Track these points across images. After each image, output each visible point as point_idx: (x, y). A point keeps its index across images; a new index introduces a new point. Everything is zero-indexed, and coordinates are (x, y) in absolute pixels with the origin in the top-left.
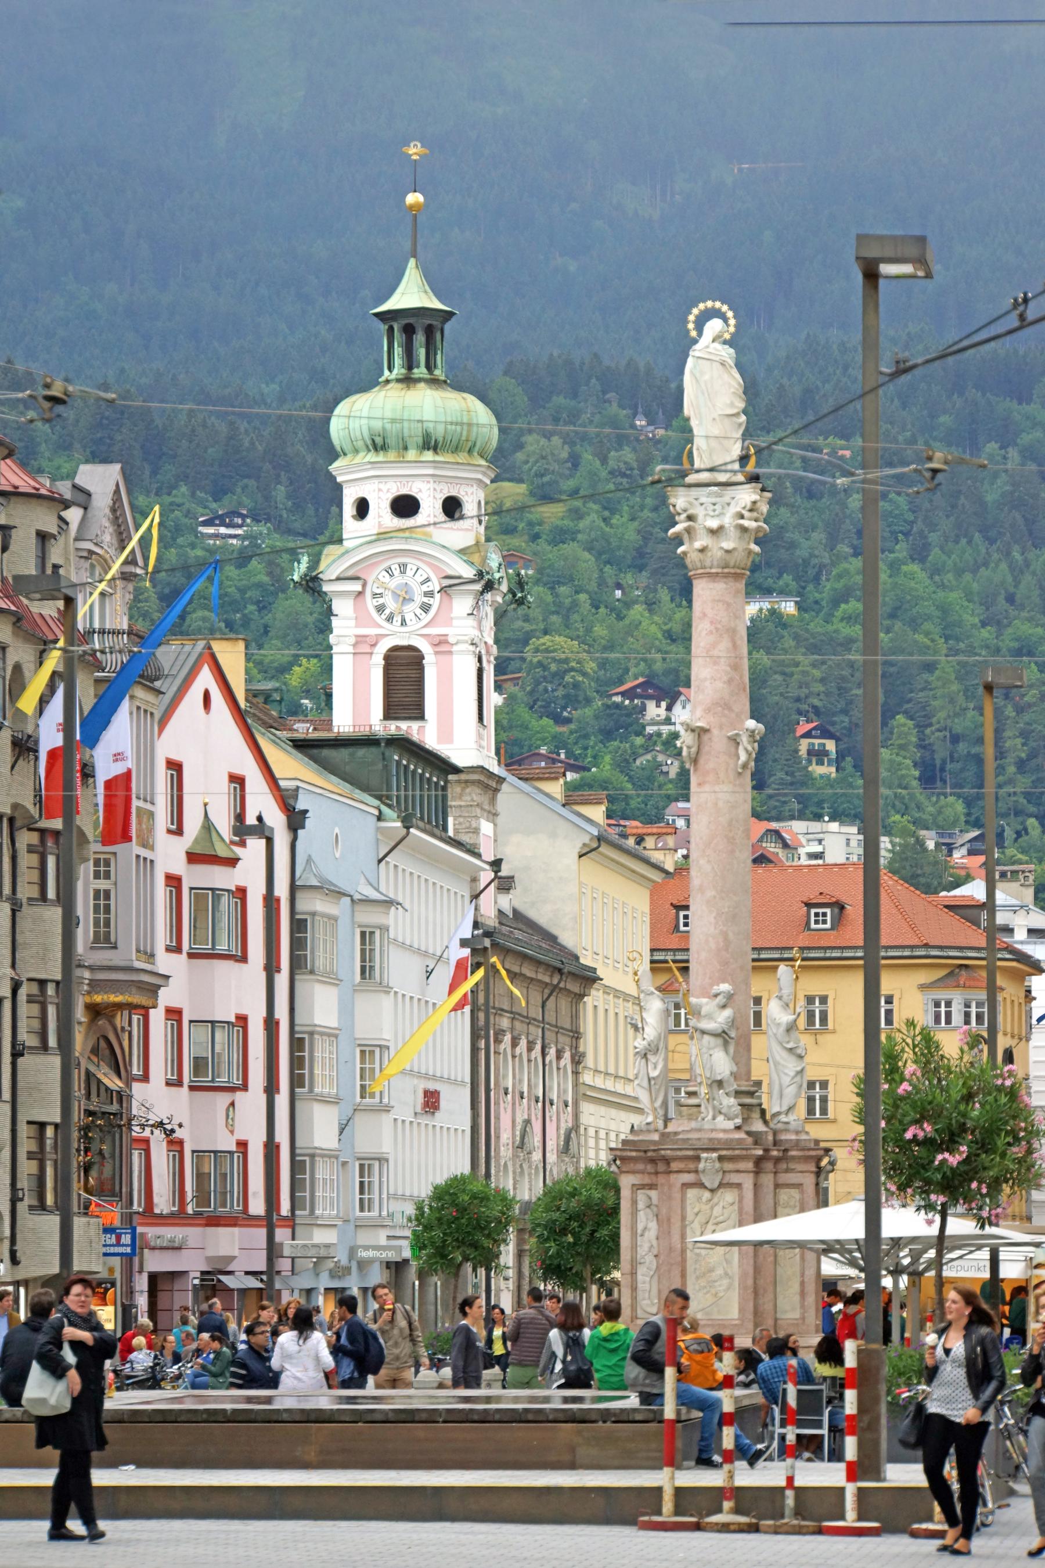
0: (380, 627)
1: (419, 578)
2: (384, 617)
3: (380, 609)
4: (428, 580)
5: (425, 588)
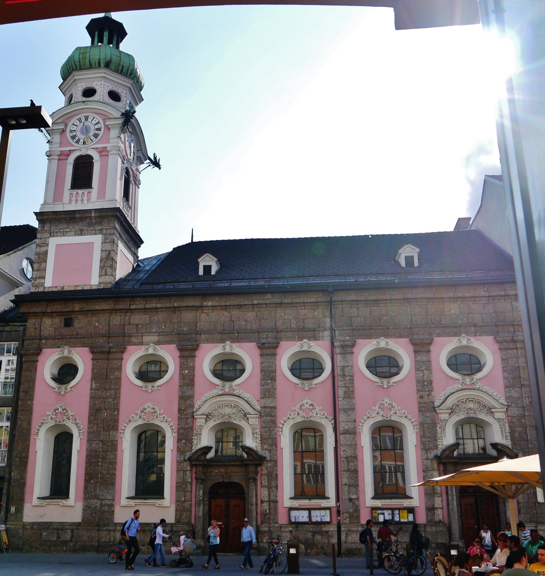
0: (73, 146)
1: (94, 122)
2: (75, 141)
3: (73, 137)
4: (98, 123)
5: (97, 127)
